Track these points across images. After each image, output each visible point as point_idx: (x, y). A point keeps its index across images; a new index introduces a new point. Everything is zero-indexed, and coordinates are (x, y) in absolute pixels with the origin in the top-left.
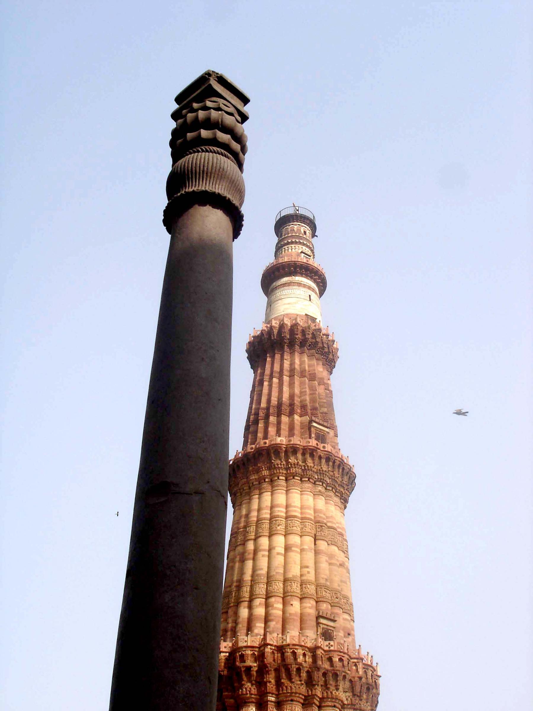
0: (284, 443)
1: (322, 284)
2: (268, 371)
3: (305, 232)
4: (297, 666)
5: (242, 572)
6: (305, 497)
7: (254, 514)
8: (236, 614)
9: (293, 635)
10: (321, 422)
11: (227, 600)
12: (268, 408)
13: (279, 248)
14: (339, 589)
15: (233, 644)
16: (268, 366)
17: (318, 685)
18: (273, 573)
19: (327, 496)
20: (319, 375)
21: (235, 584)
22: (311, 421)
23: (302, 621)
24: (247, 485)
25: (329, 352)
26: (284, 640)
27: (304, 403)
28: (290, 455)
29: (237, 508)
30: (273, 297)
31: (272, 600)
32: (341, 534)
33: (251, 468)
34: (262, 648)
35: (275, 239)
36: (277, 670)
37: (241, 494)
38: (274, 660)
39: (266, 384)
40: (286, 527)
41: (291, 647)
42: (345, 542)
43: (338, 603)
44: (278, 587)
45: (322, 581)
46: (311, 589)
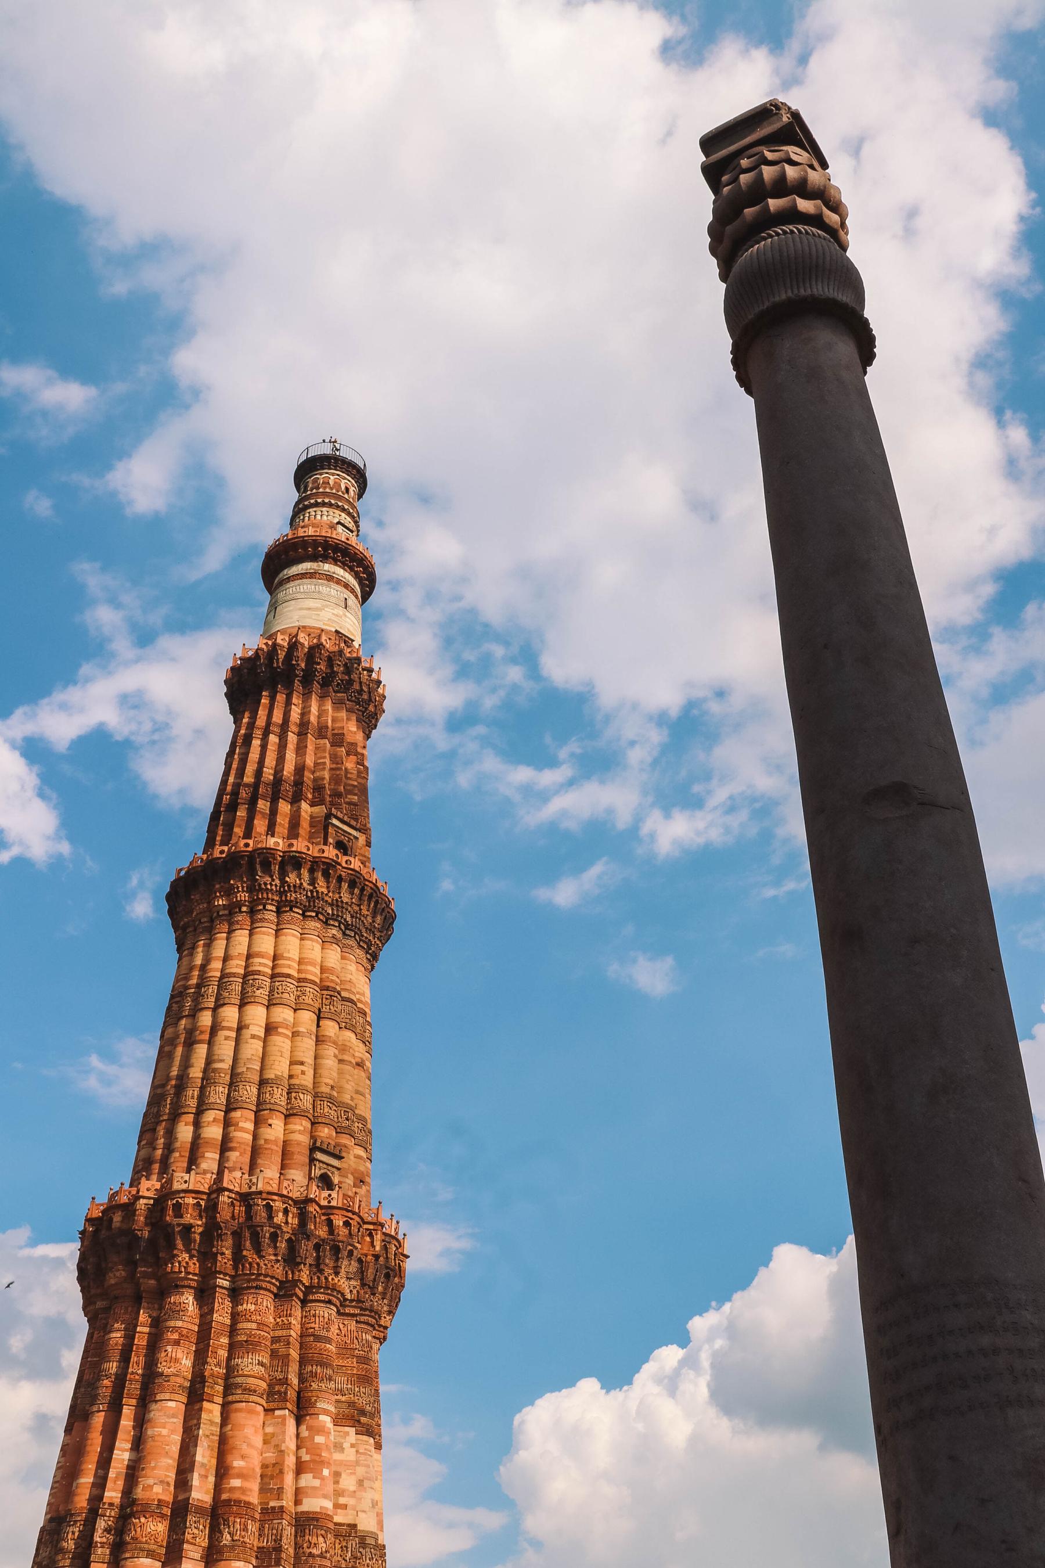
0: (280, 848)
3: (347, 490)
4: (272, 1230)
5: (186, 1064)
6: (308, 943)
7: (216, 965)
8: (170, 1134)
9: (268, 1176)
10: (346, 818)
11: (156, 1110)
12: (256, 785)
13: (299, 510)
14: (353, 1104)
15: (162, 1186)
16: (262, 714)
17: (305, 1264)
19: (345, 946)
20: (349, 738)
21: (173, 1082)
22: (329, 816)
23: (285, 1154)
24: (207, 914)
25: (370, 700)
26: (253, 1184)
27: (321, 782)
28: (289, 868)
29: (186, 952)
30: (281, 595)
31: (236, 1114)
33: (217, 886)
34: (214, 1196)
35: (295, 496)
36: (237, 1235)
37: (195, 930)
38: (233, 1217)
39: (256, 743)
40: (271, 991)
41: (264, 1196)
42: (368, 1027)
43: (348, 1127)
44: (249, 1092)
45: (325, 1089)
46: (305, 1101)
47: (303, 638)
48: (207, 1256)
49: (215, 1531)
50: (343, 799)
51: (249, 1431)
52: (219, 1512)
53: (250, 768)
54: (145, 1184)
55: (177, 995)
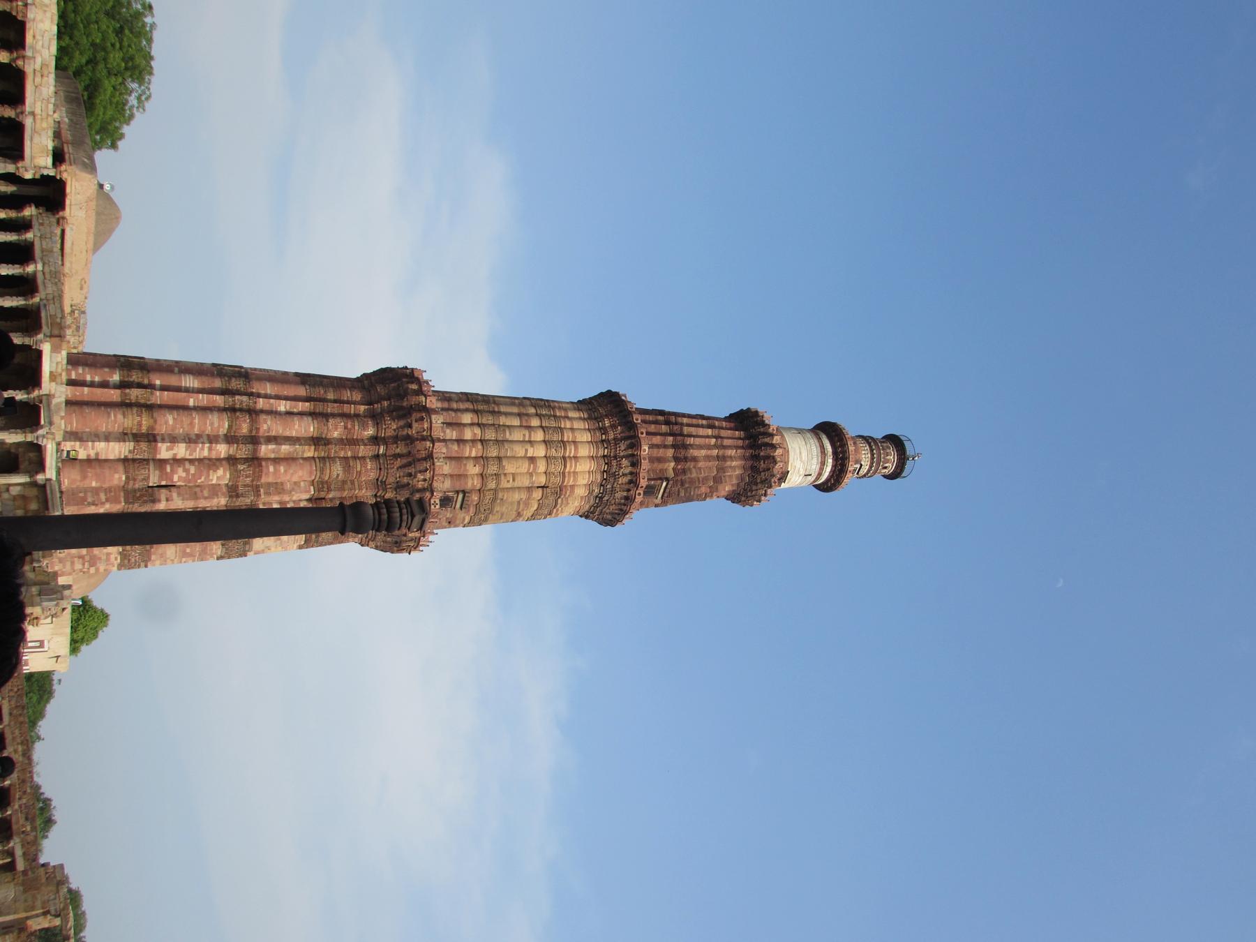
1: (827, 487)
2: (724, 433)
5: (506, 414)
7: (568, 425)
8: (467, 410)
9: (445, 468)
13: (868, 440)
18: (506, 445)
20: (720, 487)
22: (667, 480)
30: (808, 435)
31: (480, 446)
32: (550, 514)
35: (878, 435)
39: (709, 432)
44: (493, 452)
45: (500, 495)
46: (492, 485)
47: (779, 452)
48: (396, 439)
49: (246, 460)
50: (679, 488)
51: (300, 473)
52: (255, 461)
53: (693, 430)
54: (434, 399)
55: (547, 404)
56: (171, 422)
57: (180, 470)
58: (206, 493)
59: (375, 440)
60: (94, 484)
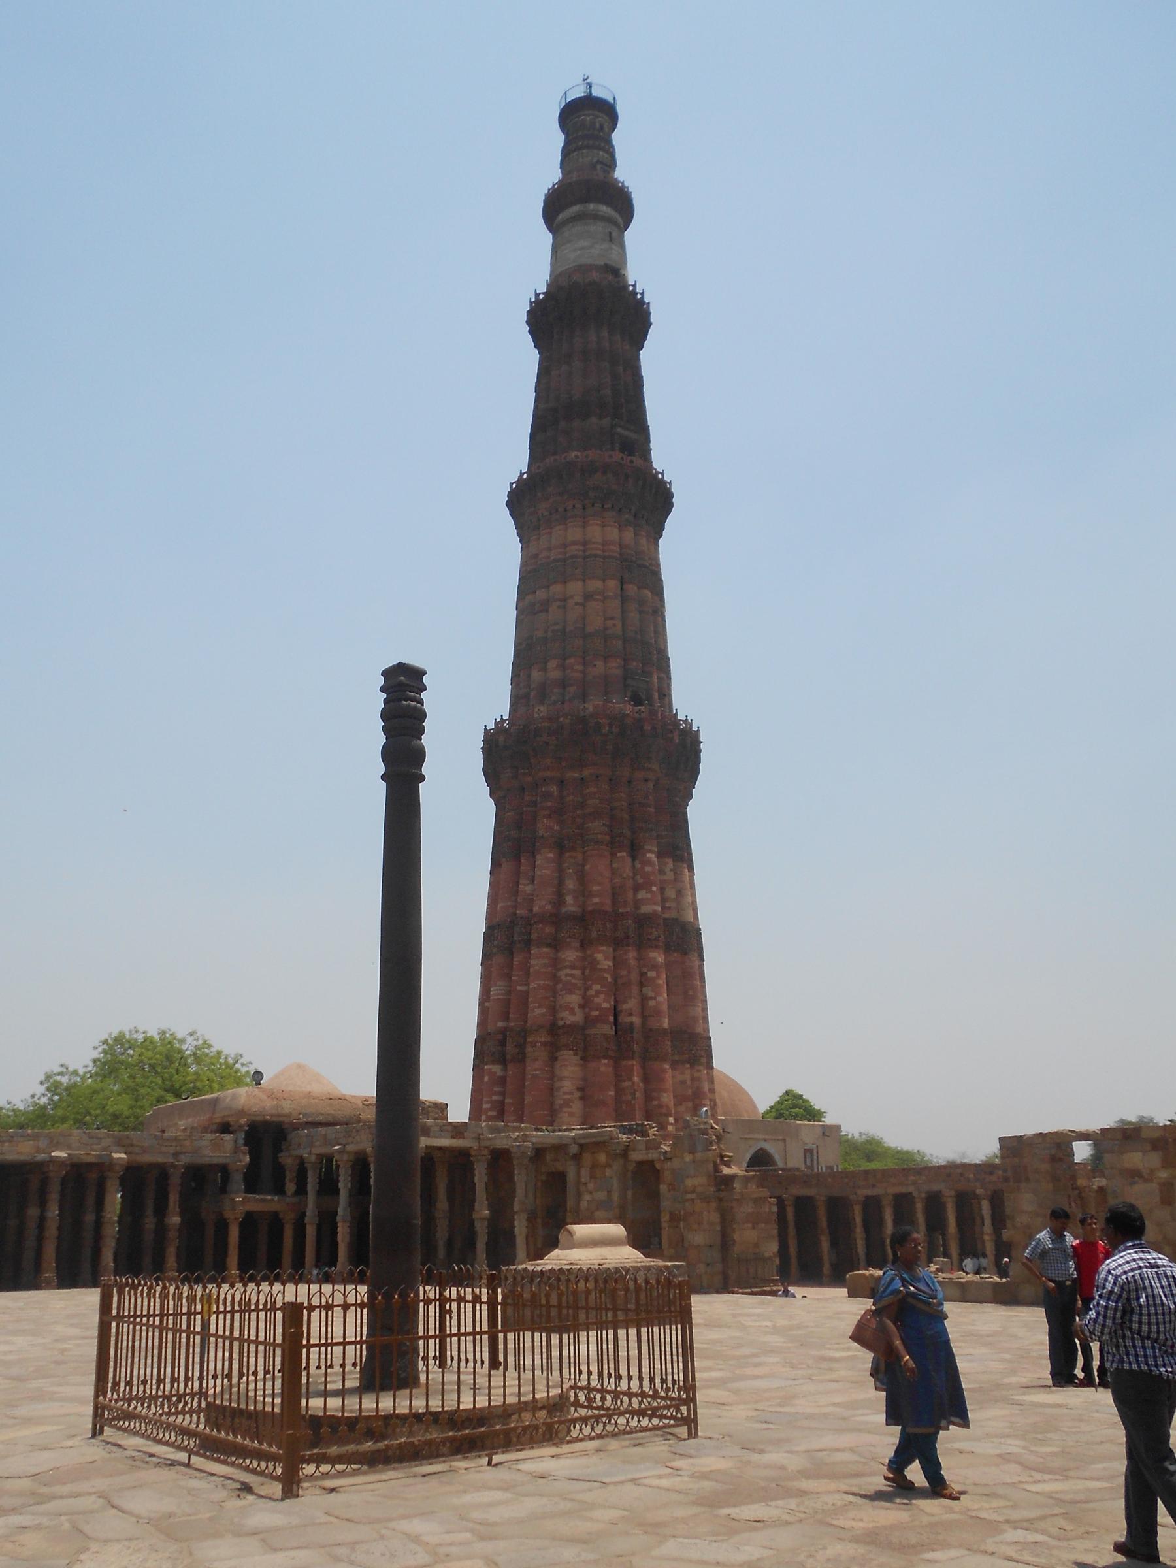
8: (529, 676)
31: (572, 660)
33: (539, 494)
56: (544, 1010)
57: (596, 1000)
58: (624, 973)
59: (561, 783)
60: (612, 1093)
